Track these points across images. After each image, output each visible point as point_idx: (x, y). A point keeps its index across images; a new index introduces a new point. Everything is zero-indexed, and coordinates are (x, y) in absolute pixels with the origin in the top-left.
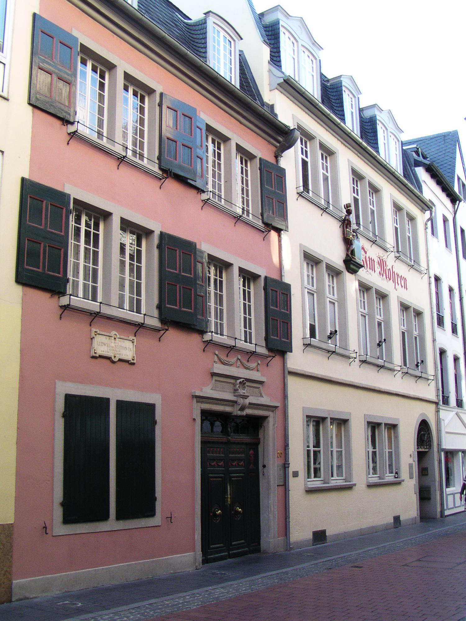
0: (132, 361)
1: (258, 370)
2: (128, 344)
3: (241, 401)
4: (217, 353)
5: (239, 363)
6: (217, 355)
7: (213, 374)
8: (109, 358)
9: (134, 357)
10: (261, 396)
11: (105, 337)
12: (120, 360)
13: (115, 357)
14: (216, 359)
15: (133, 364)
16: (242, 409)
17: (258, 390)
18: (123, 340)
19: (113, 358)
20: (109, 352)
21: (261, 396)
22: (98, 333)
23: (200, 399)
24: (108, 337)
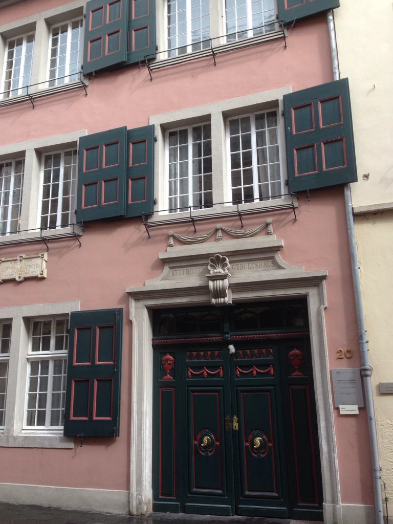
0: (39, 276)
1: (268, 234)
2: (39, 261)
3: (211, 284)
4: (171, 232)
5: (220, 233)
6: (173, 236)
7: (165, 262)
8: (13, 281)
9: (42, 272)
10: (280, 267)
11: (10, 263)
12: (27, 279)
13: (20, 277)
14: (171, 241)
15: (43, 279)
16: (220, 293)
17: (271, 261)
18: (31, 259)
19: (17, 279)
20: (12, 275)
21: (280, 267)
22: (2, 260)
23: (138, 296)
24: (13, 262)
